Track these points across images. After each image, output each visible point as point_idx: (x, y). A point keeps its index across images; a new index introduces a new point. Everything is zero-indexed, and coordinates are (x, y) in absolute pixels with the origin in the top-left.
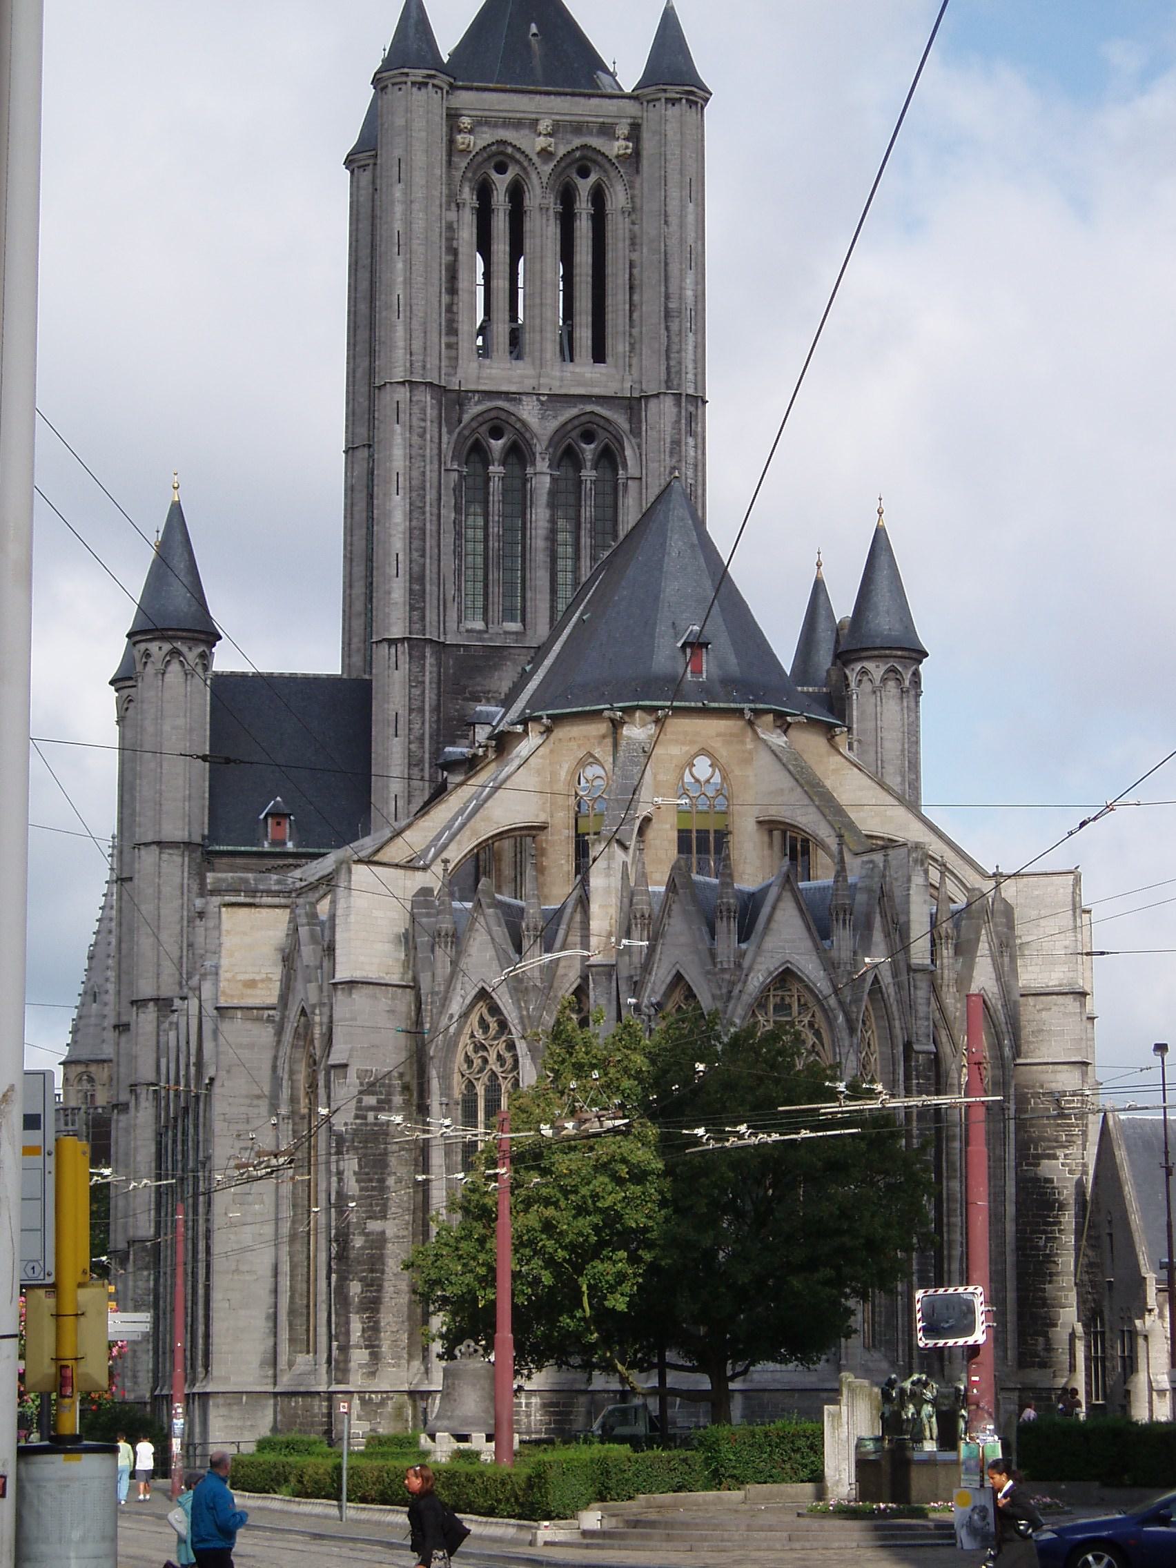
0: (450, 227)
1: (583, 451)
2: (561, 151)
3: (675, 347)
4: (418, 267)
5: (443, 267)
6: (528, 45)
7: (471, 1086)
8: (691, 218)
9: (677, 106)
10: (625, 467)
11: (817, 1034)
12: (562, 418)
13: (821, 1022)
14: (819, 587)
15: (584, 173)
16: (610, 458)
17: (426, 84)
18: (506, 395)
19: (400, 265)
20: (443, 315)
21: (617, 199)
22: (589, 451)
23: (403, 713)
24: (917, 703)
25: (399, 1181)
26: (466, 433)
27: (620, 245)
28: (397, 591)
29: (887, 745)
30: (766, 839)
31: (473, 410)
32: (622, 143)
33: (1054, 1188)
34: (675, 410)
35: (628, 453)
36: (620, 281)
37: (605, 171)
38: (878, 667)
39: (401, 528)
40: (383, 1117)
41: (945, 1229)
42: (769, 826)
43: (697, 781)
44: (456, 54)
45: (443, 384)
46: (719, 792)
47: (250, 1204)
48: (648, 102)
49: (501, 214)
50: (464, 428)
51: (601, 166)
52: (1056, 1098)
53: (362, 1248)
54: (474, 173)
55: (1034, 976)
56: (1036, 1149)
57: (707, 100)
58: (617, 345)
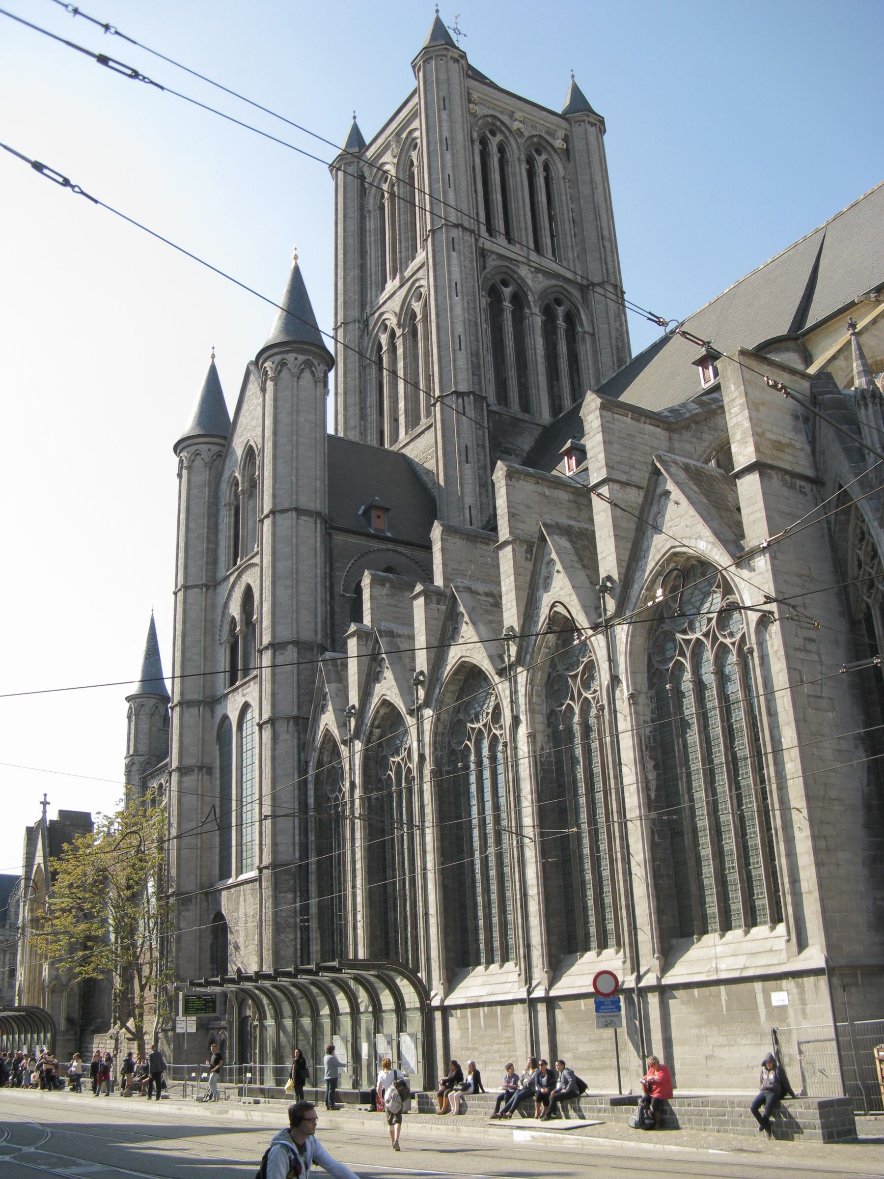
1: (556, 310)
10: (582, 326)
15: (539, 153)
16: (571, 319)
22: (560, 311)
35: (583, 317)
37: (550, 155)
39: (461, 319)
51: (548, 152)
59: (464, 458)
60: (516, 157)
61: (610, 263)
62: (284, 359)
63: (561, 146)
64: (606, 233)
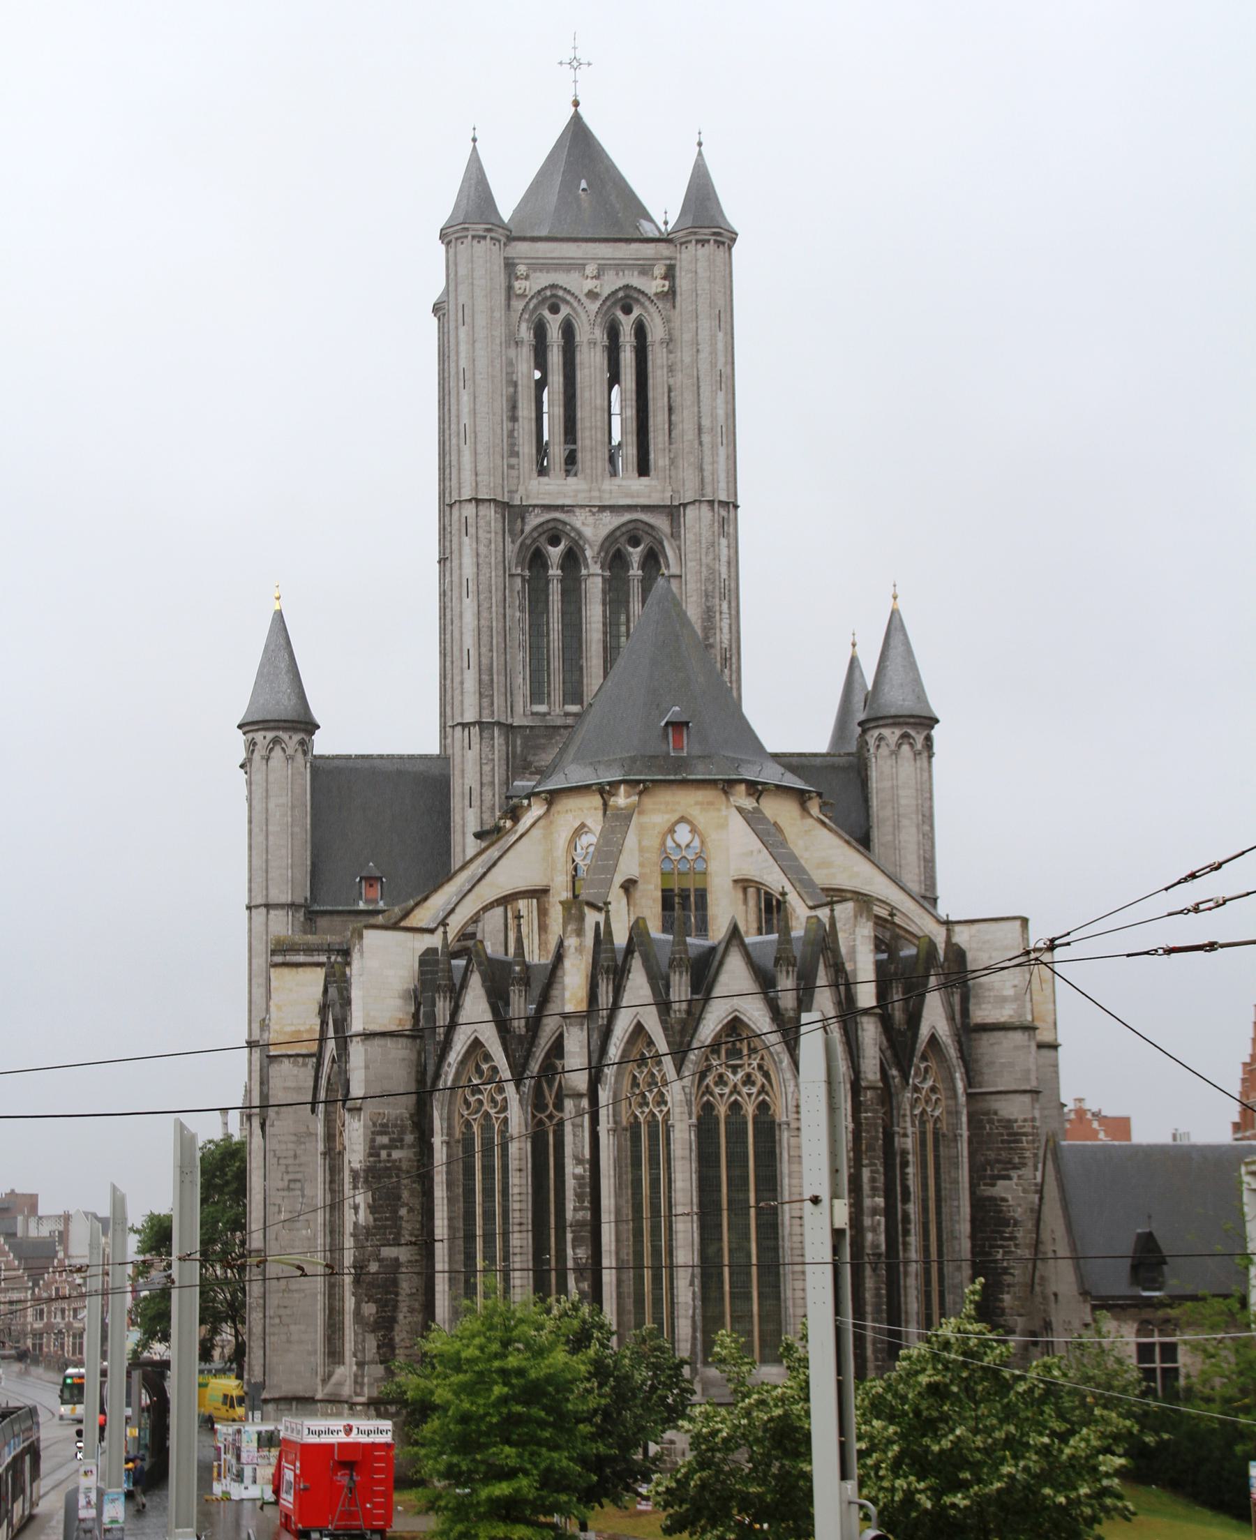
0: (510, 363)
1: (630, 554)
2: (606, 292)
3: (707, 459)
4: (482, 399)
5: (505, 398)
6: (577, 198)
7: (468, 1125)
8: (720, 346)
9: (706, 245)
10: (668, 566)
11: (766, 1075)
12: (611, 527)
13: (768, 1064)
14: (854, 663)
15: (627, 310)
16: (653, 559)
17: (484, 238)
18: (561, 508)
19: (465, 397)
20: (505, 440)
21: (656, 332)
23: (476, 787)
24: (930, 762)
25: (411, 1210)
26: (528, 542)
27: (659, 373)
28: (470, 681)
29: (903, 801)
30: (740, 895)
31: (534, 520)
32: (659, 282)
33: (1010, 1206)
34: (710, 514)
35: (670, 553)
36: (659, 404)
37: (645, 308)
38: (893, 733)
40: (396, 1154)
41: (901, 1247)
42: (744, 884)
43: (679, 846)
44: (516, 211)
45: (506, 500)
46: (699, 857)
47: (298, 1230)
48: (681, 244)
49: (555, 349)
50: (525, 538)
51: (642, 305)
52: (1008, 1123)
53: (377, 1273)
54: (531, 316)
55: (986, 1013)
56: (992, 1170)
57: (734, 240)
58: (658, 458)
59: (467, 802)
61: (707, 467)
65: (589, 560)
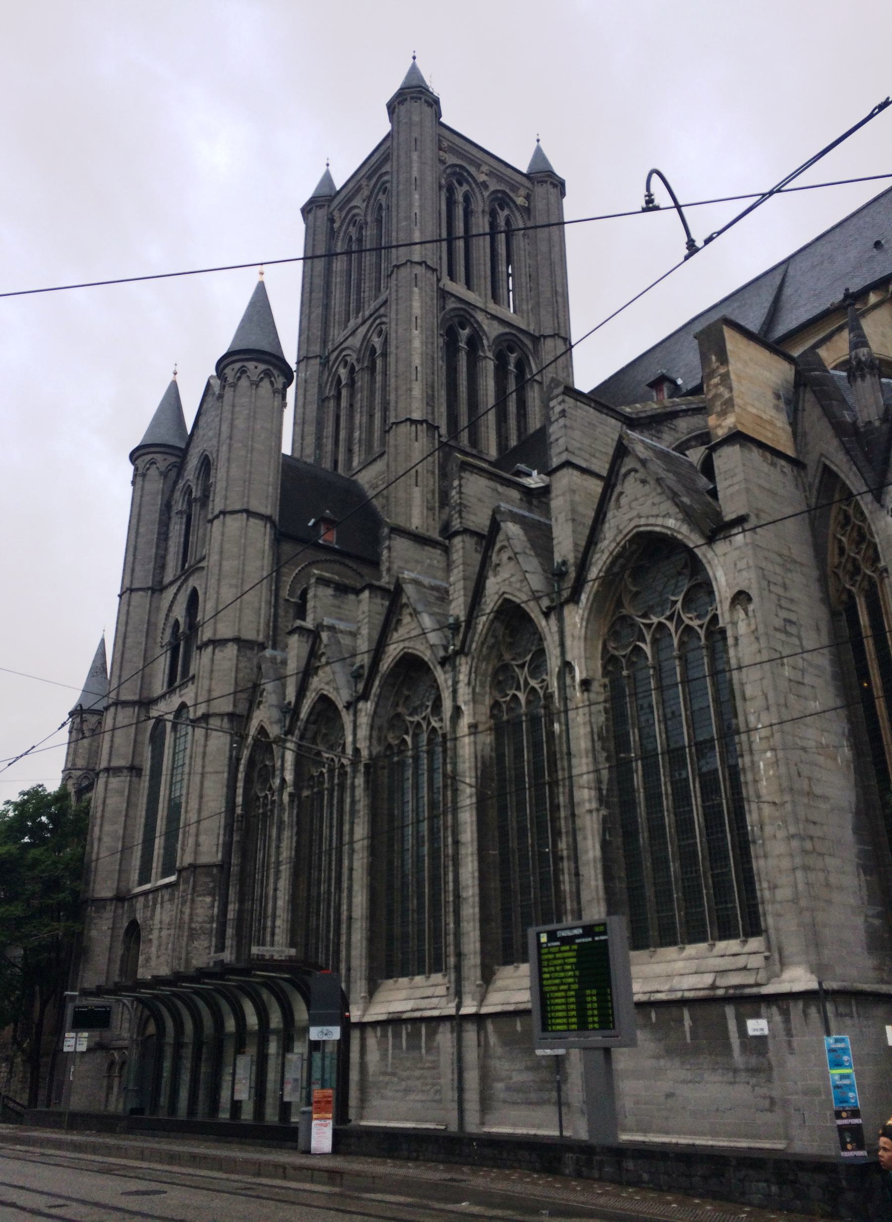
1: (509, 357)
16: (521, 365)
19: (417, 196)
22: (513, 357)
37: (512, 211)
39: (419, 351)
48: (538, 182)
51: (510, 208)
60: (480, 209)
62: (244, 366)
63: (522, 204)
64: (559, 290)
65: (486, 348)
